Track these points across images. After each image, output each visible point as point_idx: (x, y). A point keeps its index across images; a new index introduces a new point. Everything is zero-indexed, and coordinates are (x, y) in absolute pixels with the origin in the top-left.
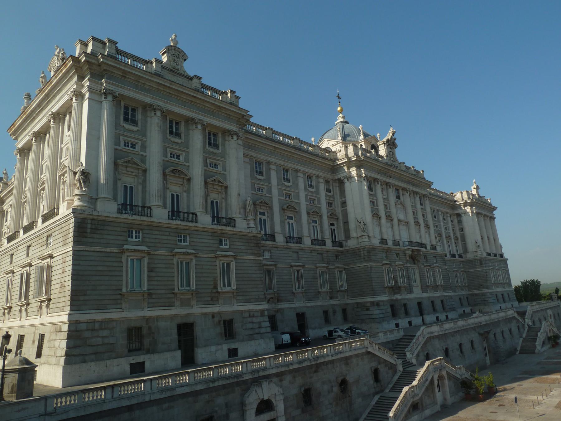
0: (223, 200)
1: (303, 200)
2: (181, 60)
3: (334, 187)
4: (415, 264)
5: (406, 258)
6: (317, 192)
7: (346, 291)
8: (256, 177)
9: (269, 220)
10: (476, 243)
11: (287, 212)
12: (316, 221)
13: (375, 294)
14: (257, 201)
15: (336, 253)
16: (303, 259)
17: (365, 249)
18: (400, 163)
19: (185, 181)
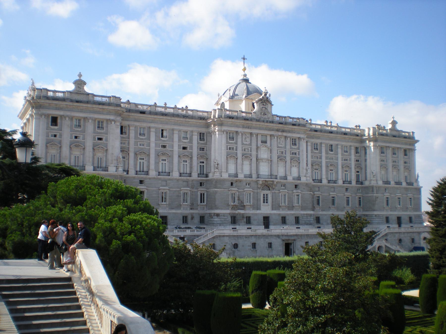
0: (104, 157)
1: (176, 148)
2: (83, 85)
3: (208, 137)
4: (269, 190)
5: (258, 186)
6: (191, 141)
7: (206, 205)
8: (139, 138)
9: (146, 162)
10: (373, 173)
11: (162, 157)
12: (187, 161)
13: (217, 209)
14: (138, 151)
15: (201, 182)
16: (170, 185)
17: (215, 180)
18: (273, 115)
19: (82, 149)
